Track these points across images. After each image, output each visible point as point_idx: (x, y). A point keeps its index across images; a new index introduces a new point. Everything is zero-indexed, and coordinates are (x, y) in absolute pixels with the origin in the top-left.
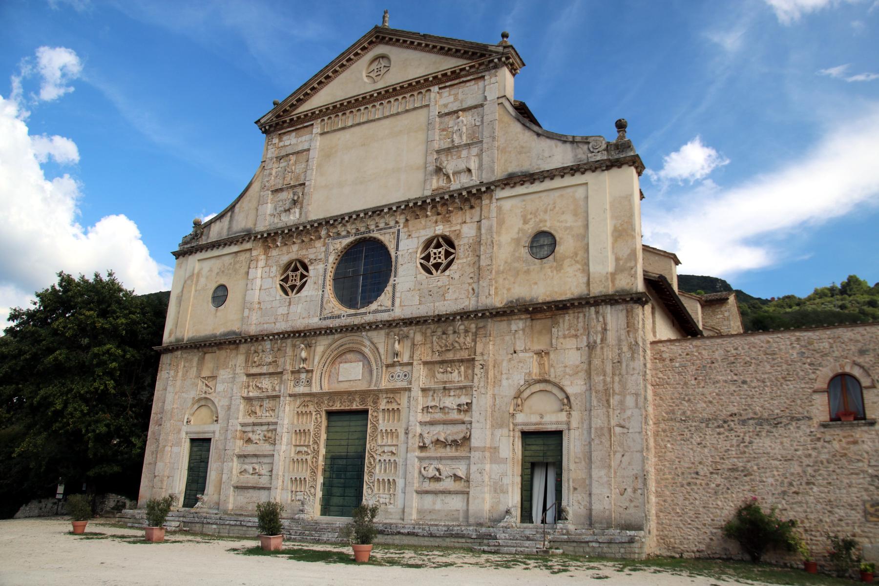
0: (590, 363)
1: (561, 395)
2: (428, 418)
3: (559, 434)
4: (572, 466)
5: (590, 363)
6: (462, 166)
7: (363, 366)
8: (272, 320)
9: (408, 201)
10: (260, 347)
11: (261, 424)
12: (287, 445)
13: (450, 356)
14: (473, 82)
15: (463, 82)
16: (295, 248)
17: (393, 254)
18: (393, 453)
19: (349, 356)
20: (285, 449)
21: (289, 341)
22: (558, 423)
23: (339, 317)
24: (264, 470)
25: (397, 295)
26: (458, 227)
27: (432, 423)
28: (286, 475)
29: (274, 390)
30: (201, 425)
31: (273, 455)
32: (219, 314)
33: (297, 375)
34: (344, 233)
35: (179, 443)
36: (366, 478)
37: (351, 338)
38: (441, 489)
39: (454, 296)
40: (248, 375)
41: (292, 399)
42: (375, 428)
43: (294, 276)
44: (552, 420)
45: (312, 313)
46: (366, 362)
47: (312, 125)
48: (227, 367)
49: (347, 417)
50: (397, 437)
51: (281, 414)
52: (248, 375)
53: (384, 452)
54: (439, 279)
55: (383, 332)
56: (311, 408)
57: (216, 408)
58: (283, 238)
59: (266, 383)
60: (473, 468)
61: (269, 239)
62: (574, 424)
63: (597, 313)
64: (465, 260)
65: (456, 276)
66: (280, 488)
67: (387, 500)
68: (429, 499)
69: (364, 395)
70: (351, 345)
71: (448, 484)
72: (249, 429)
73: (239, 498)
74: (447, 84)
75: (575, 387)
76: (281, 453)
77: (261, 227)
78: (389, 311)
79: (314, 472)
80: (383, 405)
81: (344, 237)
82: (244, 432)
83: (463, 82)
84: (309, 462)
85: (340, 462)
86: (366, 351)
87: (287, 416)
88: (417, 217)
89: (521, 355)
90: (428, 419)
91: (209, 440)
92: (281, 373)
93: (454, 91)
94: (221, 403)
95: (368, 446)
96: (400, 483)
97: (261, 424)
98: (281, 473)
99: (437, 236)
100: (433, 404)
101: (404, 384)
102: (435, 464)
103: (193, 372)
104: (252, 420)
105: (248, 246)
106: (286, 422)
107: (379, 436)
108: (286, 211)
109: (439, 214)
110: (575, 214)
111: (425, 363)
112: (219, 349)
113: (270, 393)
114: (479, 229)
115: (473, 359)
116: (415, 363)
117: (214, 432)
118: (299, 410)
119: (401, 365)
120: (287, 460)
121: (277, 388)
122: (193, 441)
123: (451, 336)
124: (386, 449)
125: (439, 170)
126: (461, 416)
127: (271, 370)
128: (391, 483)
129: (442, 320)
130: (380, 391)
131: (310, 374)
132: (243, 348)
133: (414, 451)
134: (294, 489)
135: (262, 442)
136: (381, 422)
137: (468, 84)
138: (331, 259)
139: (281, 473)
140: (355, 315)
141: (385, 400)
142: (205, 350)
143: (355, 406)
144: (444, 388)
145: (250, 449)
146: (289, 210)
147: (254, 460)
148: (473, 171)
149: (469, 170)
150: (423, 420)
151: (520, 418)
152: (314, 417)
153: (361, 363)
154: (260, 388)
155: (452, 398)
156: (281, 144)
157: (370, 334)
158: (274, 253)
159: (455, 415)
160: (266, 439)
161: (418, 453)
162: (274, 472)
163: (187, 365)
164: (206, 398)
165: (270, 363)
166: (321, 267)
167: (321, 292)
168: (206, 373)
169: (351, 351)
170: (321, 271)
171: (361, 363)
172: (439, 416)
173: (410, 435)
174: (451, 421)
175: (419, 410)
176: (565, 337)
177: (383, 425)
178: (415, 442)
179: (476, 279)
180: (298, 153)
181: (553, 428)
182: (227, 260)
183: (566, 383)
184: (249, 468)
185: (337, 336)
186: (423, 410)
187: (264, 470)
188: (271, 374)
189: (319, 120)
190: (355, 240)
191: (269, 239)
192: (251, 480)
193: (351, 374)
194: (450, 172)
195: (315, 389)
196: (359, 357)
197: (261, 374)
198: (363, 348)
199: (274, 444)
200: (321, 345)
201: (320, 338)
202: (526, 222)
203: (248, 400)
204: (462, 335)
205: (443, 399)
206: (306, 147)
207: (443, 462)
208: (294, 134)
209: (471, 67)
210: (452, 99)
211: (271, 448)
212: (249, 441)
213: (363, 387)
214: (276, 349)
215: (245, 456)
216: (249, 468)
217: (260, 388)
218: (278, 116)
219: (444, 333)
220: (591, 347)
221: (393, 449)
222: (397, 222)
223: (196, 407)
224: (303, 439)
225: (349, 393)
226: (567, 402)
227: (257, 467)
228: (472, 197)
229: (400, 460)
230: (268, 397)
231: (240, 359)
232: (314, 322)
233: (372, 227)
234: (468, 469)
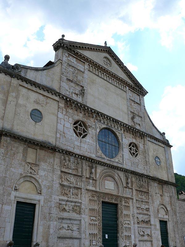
0: (171, 202)
1: (166, 210)
3: (166, 222)
4: (171, 233)
5: (171, 202)
6: (138, 122)
7: (114, 184)
8: (72, 146)
9: (127, 125)
10: (67, 158)
11: (72, 202)
13: (141, 189)
14: (136, 95)
15: (134, 92)
16: (81, 115)
17: (121, 141)
19: (109, 178)
20: (85, 218)
21: (84, 161)
22: (167, 219)
23: (104, 159)
24: (75, 228)
25: (124, 159)
26: (139, 143)
27: (140, 214)
28: (87, 231)
29: (77, 184)
30: (27, 194)
31: (80, 220)
32: (37, 126)
33: (88, 180)
34: (102, 122)
35: (9, 203)
37: (111, 170)
38: (145, 239)
39: (140, 168)
40: (62, 172)
41: (86, 191)
43: (80, 129)
44: (166, 218)
45: (92, 151)
46: (115, 183)
47: (85, 63)
48: (46, 162)
50: (130, 218)
52: (62, 172)
54: (132, 158)
55: (122, 173)
56: (96, 198)
57: (40, 185)
58: (75, 106)
59: (72, 179)
60: (153, 232)
61: (69, 102)
62: (170, 220)
63: (171, 187)
64: (142, 156)
65: (140, 160)
68: (142, 243)
69: (117, 197)
70: (110, 174)
71: (146, 238)
72: (64, 203)
73: (60, 244)
74: (131, 89)
75: (169, 209)
77: (63, 93)
78: (122, 164)
80: (123, 203)
81: (102, 123)
82: (60, 204)
83: (134, 92)
86: (116, 178)
87: (85, 200)
88: (127, 132)
89: (158, 194)
91: (34, 205)
92: (81, 176)
93: (132, 93)
94: (44, 183)
96: (133, 237)
97: (72, 202)
99: (133, 143)
100: (139, 206)
101: (130, 196)
102: (142, 229)
103: (20, 156)
104: (66, 198)
105: (57, 98)
108: (75, 94)
109: (133, 135)
110: (163, 156)
111: (136, 190)
112: (40, 149)
114: (144, 147)
115: (148, 193)
116: (134, 189)
117: (39, 201)
119: (129, 188)
121: (78, 184)
122: (18, 203)
123: (141, 182)
124: (127, 222)
125: (133, 118)
126: (146, 213)
127: (74, 173)
128: (129, 237)
129: (141, 176)
130: (123, 197)
131: (94, 182)
132: (57, 154)
134: (91, 239)
135: (71, 211)
137: (135, 94)
138: (98, 130)
140: (110, 161)
141: (124, 201)
142: (30, 145)
143: (113, 201)
144: (142, 201)
145: (65, 215)
146: (77, 95)
147: (69, 222)
148: (141, 126)
149: (139, 125)
151: (160, 216)
152: (97, 203)
153: (113, 183)
154: (69, 181)
155: (144, 205)
156: (69, 59)
157: (118, 171)
158: (70, 111)
159: (145, 212)
160: (74, 210)
163: (14, 149)
164: (31, 177)
165: (74, 169)
166: (93, 131)
167: (95, 143)
168: (29, 160)
169: (110, 176)
170: (94, 134)
171: (113, 183)
172: (141, 211)
174: (144, 213)
176: (165, 192)
177: (125, 212)
179: (145, 163)
180: (78, 70)
181: (165, 220)
182: (41, 98)
183: (167, 206)
184: (66, 226)
185: (106, 168)
187: (75, 228)
189: (88, 64)
190: (106, 128)
191: (69, 102)
192: (68, 233)
193: (109, 186)
194: (135, 122)
195: (98, 190)
196: (112, 179)
197: (69, 173)
198: (115, 177)
199: (80, 213)
200: (100, 169)
201: (98, 166)
202: (154, 152)
203: (62, 186)
204: (144, 183)
205: (142, 205)
206: (82, 70)
207: (144, 229)
208: (75, 59)
209: (138, 90)
210: (131, 95)
211: (78, 216)
212: (64, 210)
213: (115, 193)
214: (76, 163)
215: (63, 219)
216: (66, 226)
217: (69, 181)
218: (70, 46)
219: (140, 181)
220: (171, 197)
221: (129, 222)
222: (121, 130)
223: (22, 180)
225: (112, 195)
226: (167, 212)
227: (70, 225)
228: (142, 135)
230: (75, 187)
231: (57, 161)
232: (93, 156)
233: (113, 126)
234: (151, 232)
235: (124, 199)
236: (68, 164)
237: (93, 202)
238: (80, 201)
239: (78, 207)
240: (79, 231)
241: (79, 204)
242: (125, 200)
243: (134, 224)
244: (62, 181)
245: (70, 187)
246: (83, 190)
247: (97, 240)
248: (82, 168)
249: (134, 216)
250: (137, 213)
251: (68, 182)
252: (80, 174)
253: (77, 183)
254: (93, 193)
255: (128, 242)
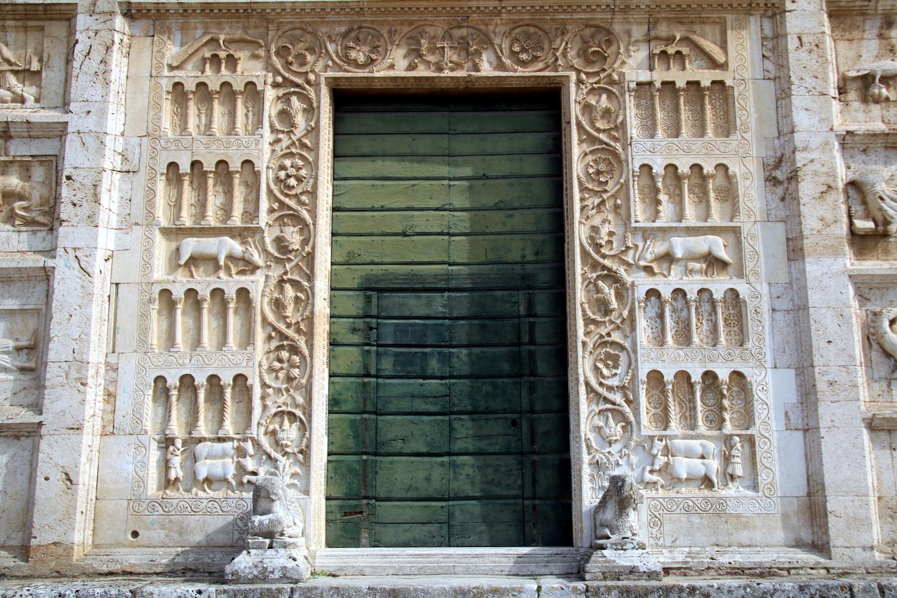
2: (870, 120)
12: (126, 224)
18: (713, 263)
28: (128, 365)
31: (46, 275)
36: (583, 366)
42: (610, 158)
49: (438, 119)
50: (729, 194)
51: (82, 86)
53: (668, 258)
56: (249, 69)
66: (93, 425)
67: (714, 465)
76: (98, 264)
79: (288, 347)
84: (262, 304)
85: (415, 304)
90: (879, 127)
95: (579, 233)
98: (96, 355)
106: (114, 124)
107: (635, 194)
118: (189, 77)
120: (130, 298)
124: (680, 245)
133: (836, 253)
134: (177, 428)
136: (634, 129)
139: (96, 355)
143: (487, 69)
150: (860, 127)
161: (848, 261)
162: (57, 351)
173: (807, 189)
175: (834, 92)
178: (823, 216)
186: (842, 90)
221: (720, 247)
224: (214, 201)
229: (757, 290)
235: (652, 23)
237: (218, 109)
238: (54, 116)
239: (38, 173)
240: (32, 365)
241: (46, 147)
242: (663, 30)
243: (795, 250)
246: (82, 21)
247: (254, 431)
249: (793, 177)
250: (847, 141)
254: (214, 32)
255: (696, 445)
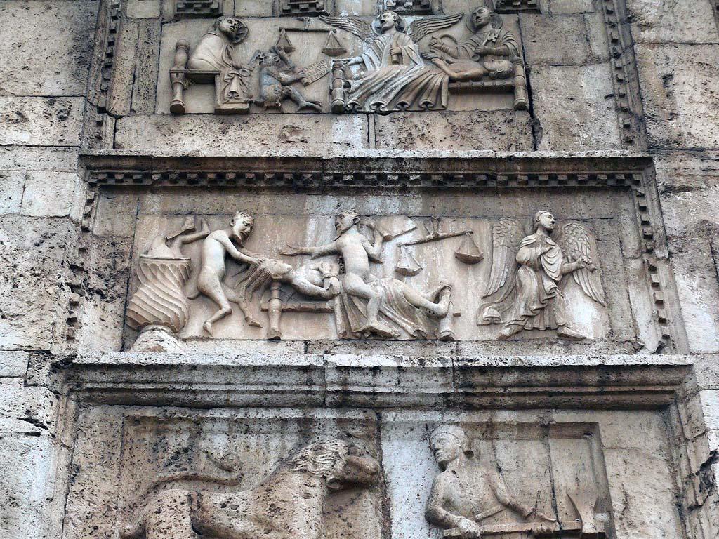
29: (542, 323)
59: (396, 260)
92: (617, 178)
113: (473, 343)
121: (581, 313)
127: (437, 140)
154: (309, 303)
188: (445, 182)
197: (299, 179)
217: (309, 303)
230: (472, 391)
236: (282, 54)
244: (132, 327)
245: (362, 408)
248: (622, 56)
251: (297, 330)
252: (603, 139)
253: (547, 303)
